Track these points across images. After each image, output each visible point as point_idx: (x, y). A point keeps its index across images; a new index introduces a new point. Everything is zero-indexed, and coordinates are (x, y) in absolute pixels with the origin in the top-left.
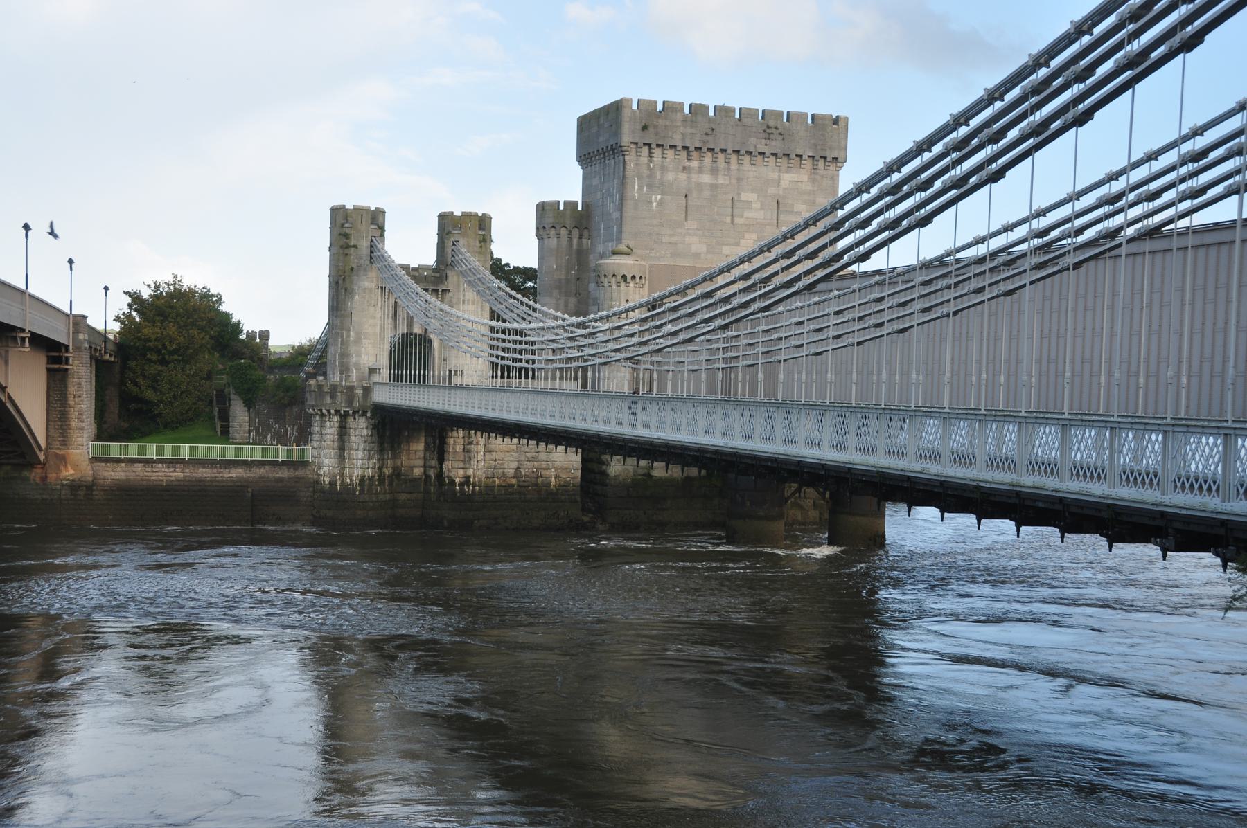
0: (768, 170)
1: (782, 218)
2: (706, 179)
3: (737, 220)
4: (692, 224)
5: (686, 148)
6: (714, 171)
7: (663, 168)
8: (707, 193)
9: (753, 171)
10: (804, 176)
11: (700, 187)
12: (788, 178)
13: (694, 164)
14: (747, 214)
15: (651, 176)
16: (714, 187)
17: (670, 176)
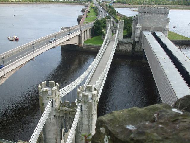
0: (158, 15)
1: (160, 21)
2: (150, 16)
3: (154, 21)
4: (148, 21)
5: (147, 12)
6: (151, 15)
7: (145, 15)
8: (150, 18)
9: (156, 15)
10: (163, 16)
11: (149, 17)
12: (161, 16)
13: (149, 14)
14: (155, 20)
15: (143, 16)
16: (151, 17)
17: (145, 16)
